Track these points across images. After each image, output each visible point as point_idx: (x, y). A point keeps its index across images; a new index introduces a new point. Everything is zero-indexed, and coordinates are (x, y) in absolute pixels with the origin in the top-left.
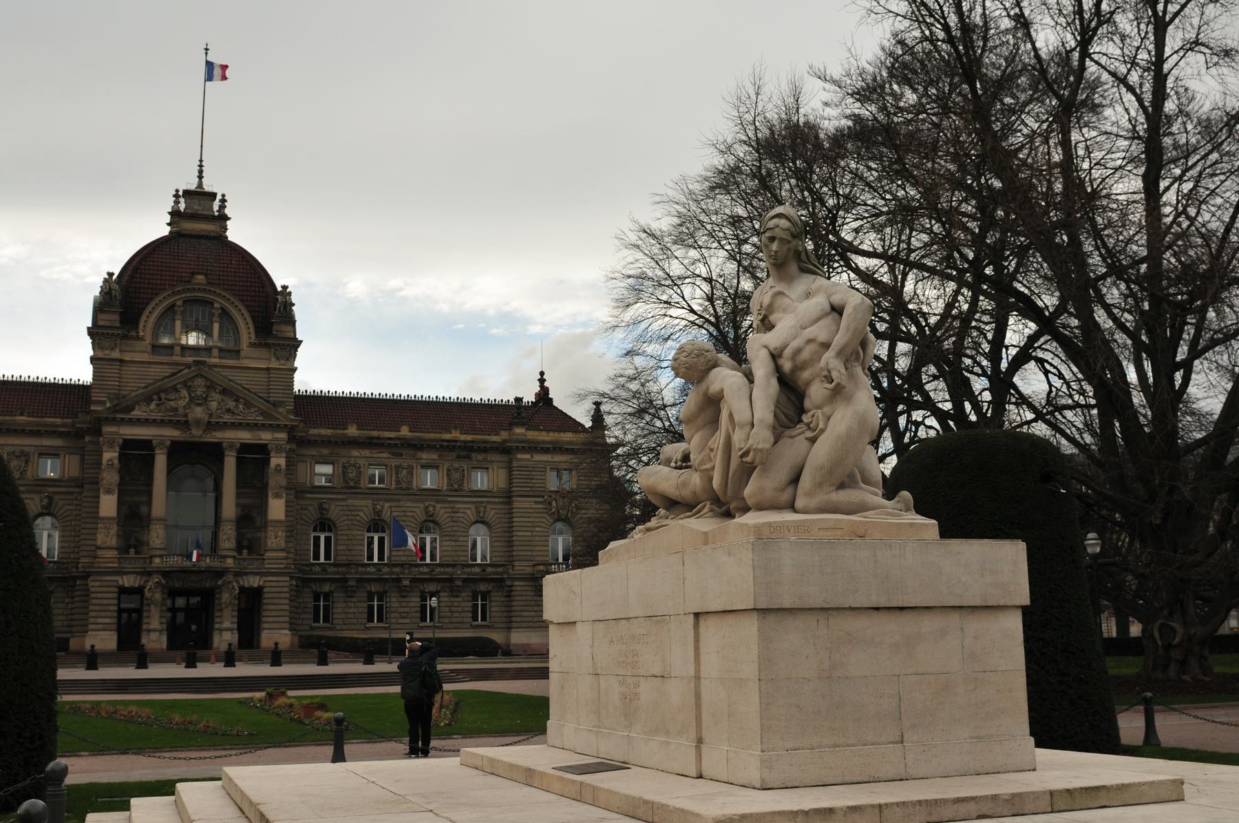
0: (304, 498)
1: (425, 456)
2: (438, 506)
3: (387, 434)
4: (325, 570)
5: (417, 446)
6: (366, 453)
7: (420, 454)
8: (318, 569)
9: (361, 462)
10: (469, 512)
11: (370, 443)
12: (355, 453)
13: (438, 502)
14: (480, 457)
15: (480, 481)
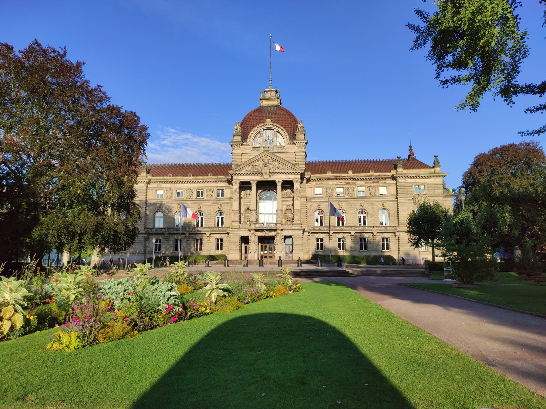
0: (311, 201)
1: (360, 182)
2: (366, 203)
3: (343, 175)
4: (320, 229)
5: (357, 179)
6: (335, 182)
7: (357, 182)
8: (317, 228)
9: (333, 187)
10: (379, 205)
11: (336, 179)
12: (331, 182)
13: (366, 201)
14: (383, 181)
15: (383, 191)
